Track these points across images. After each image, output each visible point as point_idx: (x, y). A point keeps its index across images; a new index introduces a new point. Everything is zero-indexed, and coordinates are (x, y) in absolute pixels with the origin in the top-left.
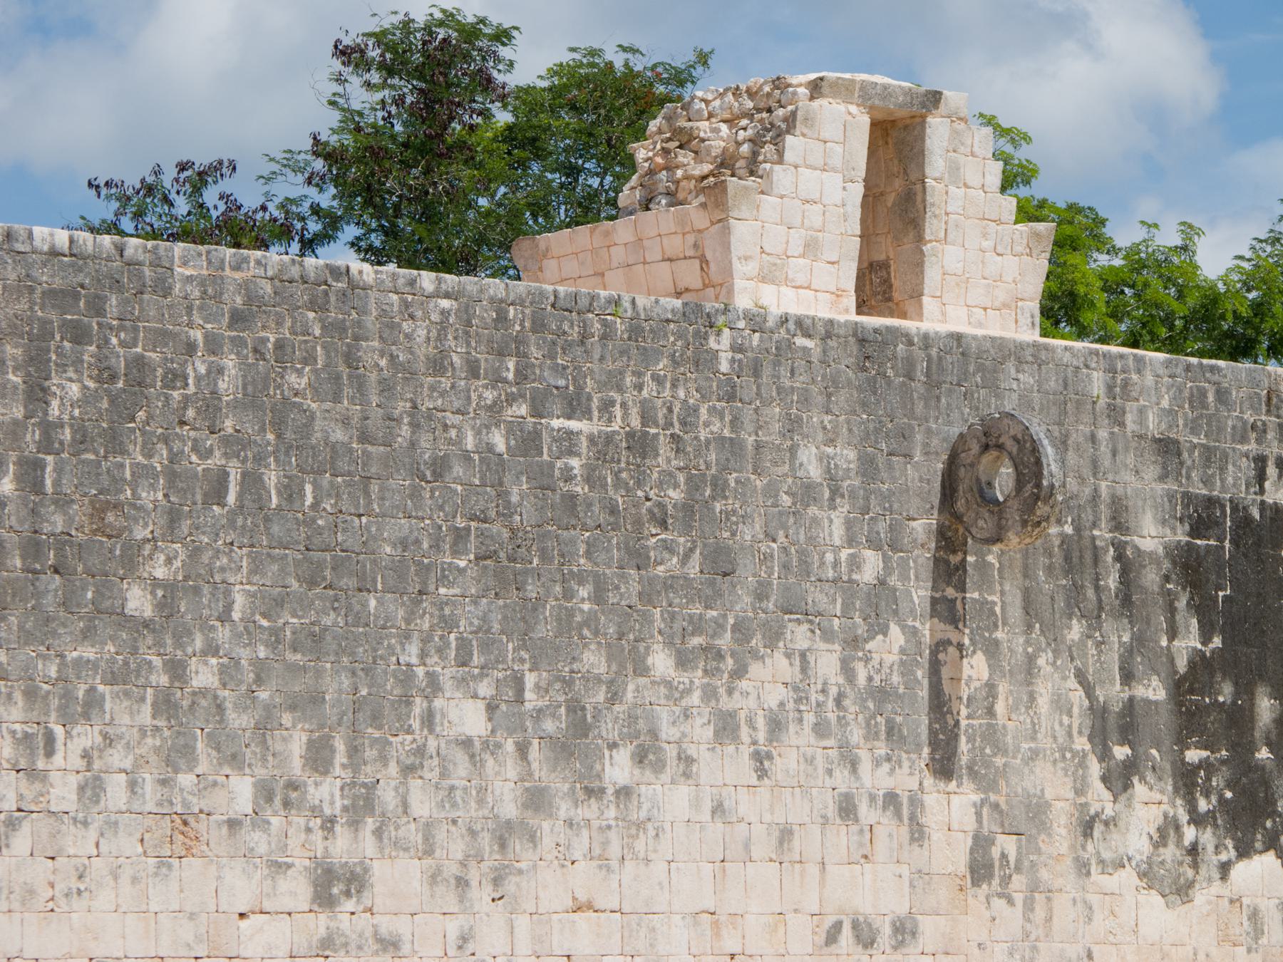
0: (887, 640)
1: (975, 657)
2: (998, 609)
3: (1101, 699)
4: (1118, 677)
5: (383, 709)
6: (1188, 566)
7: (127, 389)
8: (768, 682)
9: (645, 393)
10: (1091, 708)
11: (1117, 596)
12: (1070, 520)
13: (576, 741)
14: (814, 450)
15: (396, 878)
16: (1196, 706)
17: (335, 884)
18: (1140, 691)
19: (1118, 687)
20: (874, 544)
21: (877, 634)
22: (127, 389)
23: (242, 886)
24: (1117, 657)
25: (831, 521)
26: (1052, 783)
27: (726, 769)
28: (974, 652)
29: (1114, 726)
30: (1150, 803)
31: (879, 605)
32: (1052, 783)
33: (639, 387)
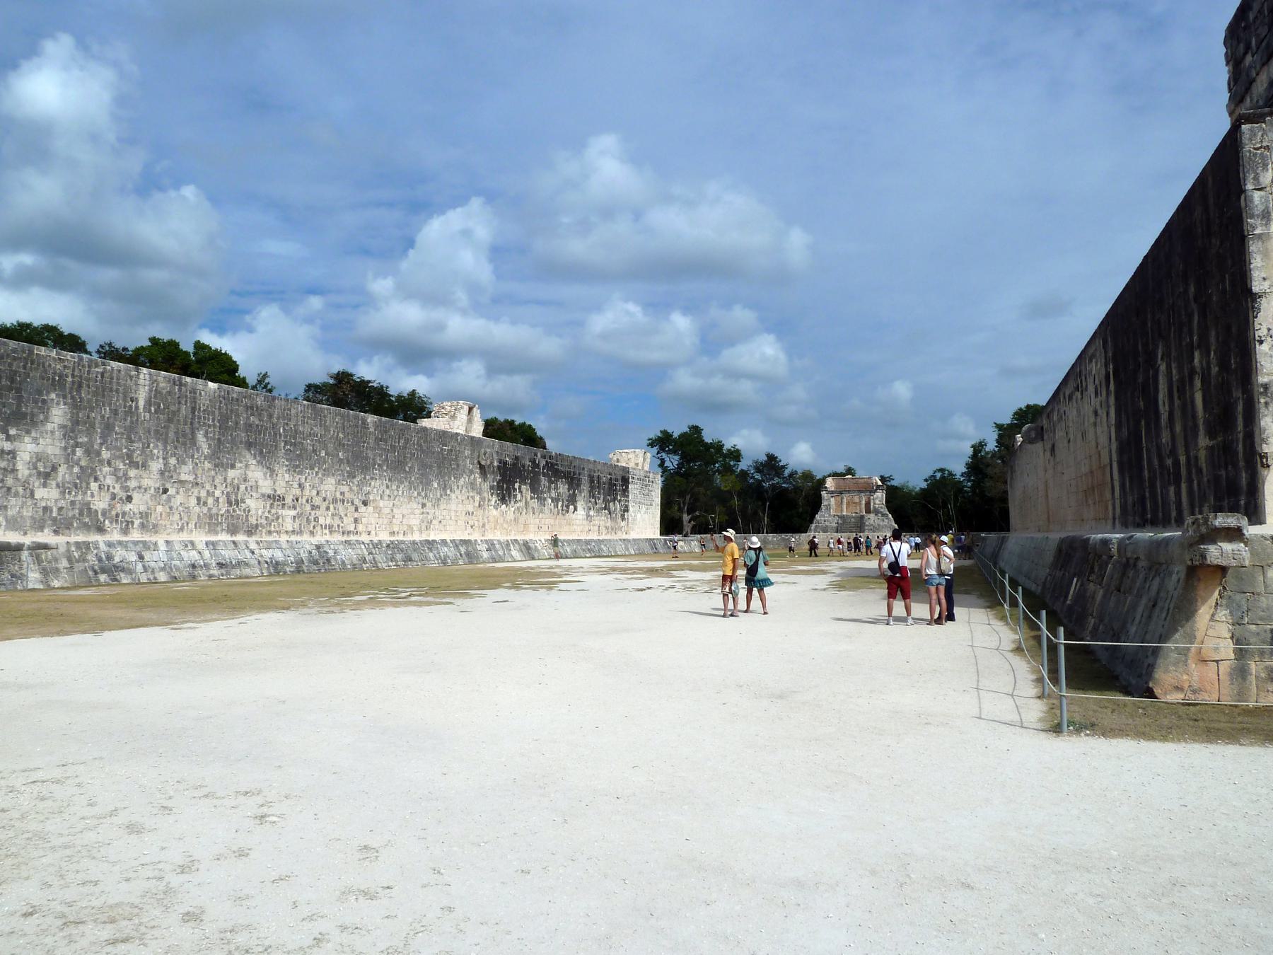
5: (428, 483)
6: (499, 467)
7: (407, 441)
8: (461, 482)
13: (445, 489)
15: (429, 504)
16: (499, 487)
17: (424, 505)
22: (407, 441)
23: (415, 506)
26: (485, 495)
27: (458, 492)
29: (492, 488)
30: (494, 498)
31: (472, 472)
32: (485, 495)
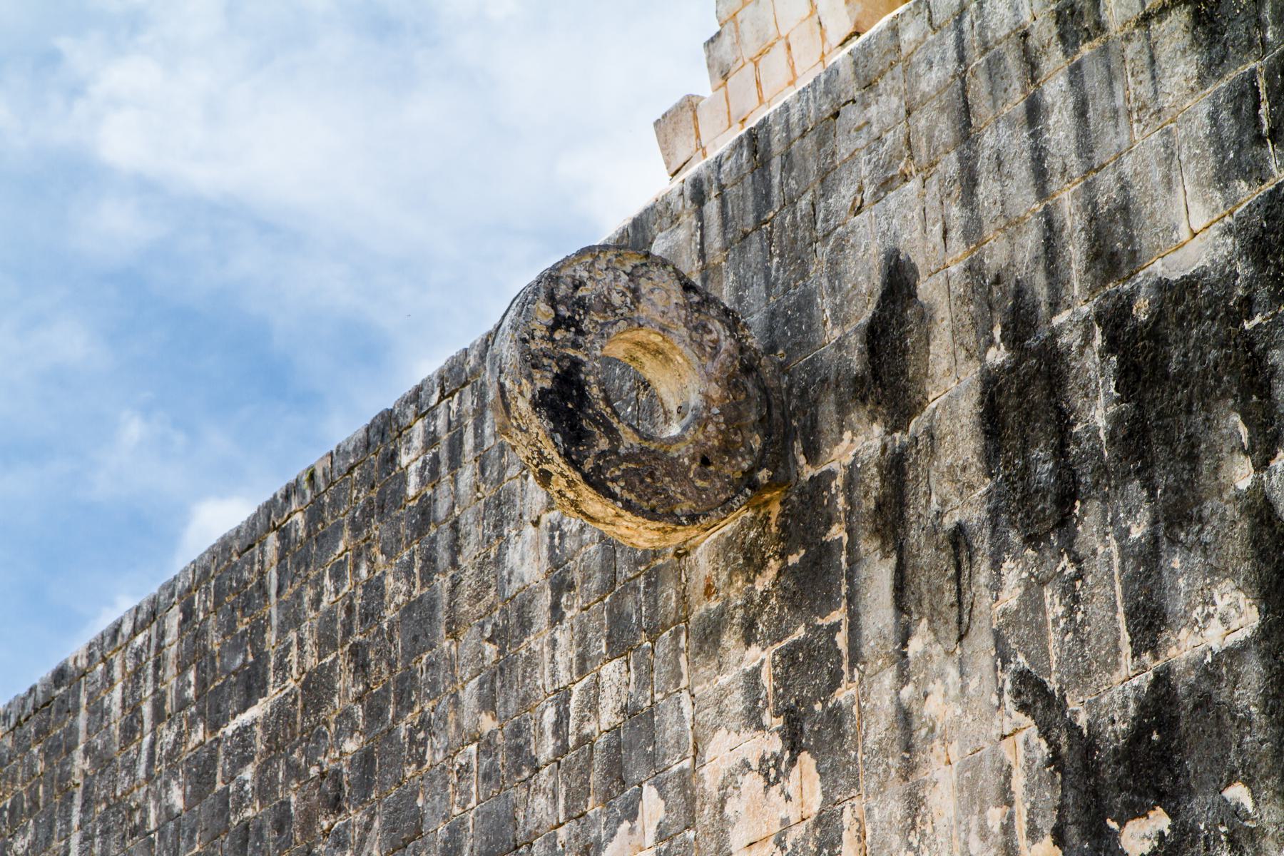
0: (638, 823)
1: (795, 772)
2: (841, 639)
3: (1082, 720)
4: (1125, 638)
9: (325, 604)
10: (1055, 759)
11: (1112, 436)
12: (997, 332)
14: (529, 531)
18: (1186, 647)
19: (1126, 662)
20: (619, 646)
21: (620, 821)
24: (1118, 587)
25: (553, 643)
28: (793, 762)
33: (316, 602)
